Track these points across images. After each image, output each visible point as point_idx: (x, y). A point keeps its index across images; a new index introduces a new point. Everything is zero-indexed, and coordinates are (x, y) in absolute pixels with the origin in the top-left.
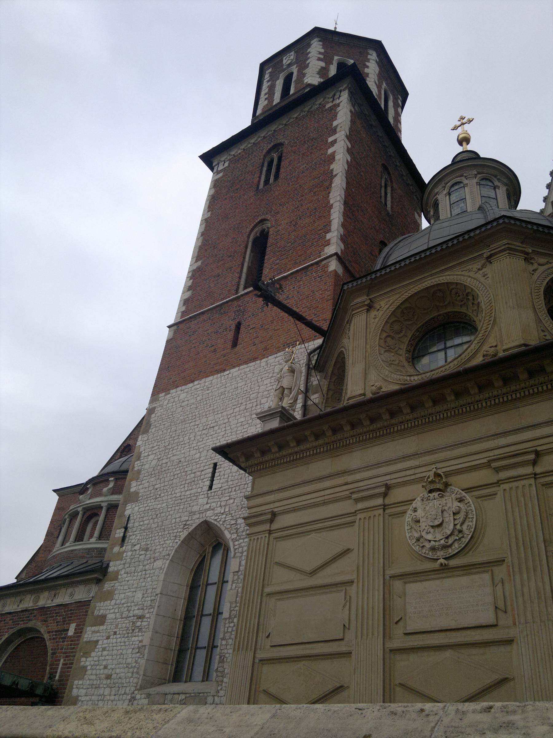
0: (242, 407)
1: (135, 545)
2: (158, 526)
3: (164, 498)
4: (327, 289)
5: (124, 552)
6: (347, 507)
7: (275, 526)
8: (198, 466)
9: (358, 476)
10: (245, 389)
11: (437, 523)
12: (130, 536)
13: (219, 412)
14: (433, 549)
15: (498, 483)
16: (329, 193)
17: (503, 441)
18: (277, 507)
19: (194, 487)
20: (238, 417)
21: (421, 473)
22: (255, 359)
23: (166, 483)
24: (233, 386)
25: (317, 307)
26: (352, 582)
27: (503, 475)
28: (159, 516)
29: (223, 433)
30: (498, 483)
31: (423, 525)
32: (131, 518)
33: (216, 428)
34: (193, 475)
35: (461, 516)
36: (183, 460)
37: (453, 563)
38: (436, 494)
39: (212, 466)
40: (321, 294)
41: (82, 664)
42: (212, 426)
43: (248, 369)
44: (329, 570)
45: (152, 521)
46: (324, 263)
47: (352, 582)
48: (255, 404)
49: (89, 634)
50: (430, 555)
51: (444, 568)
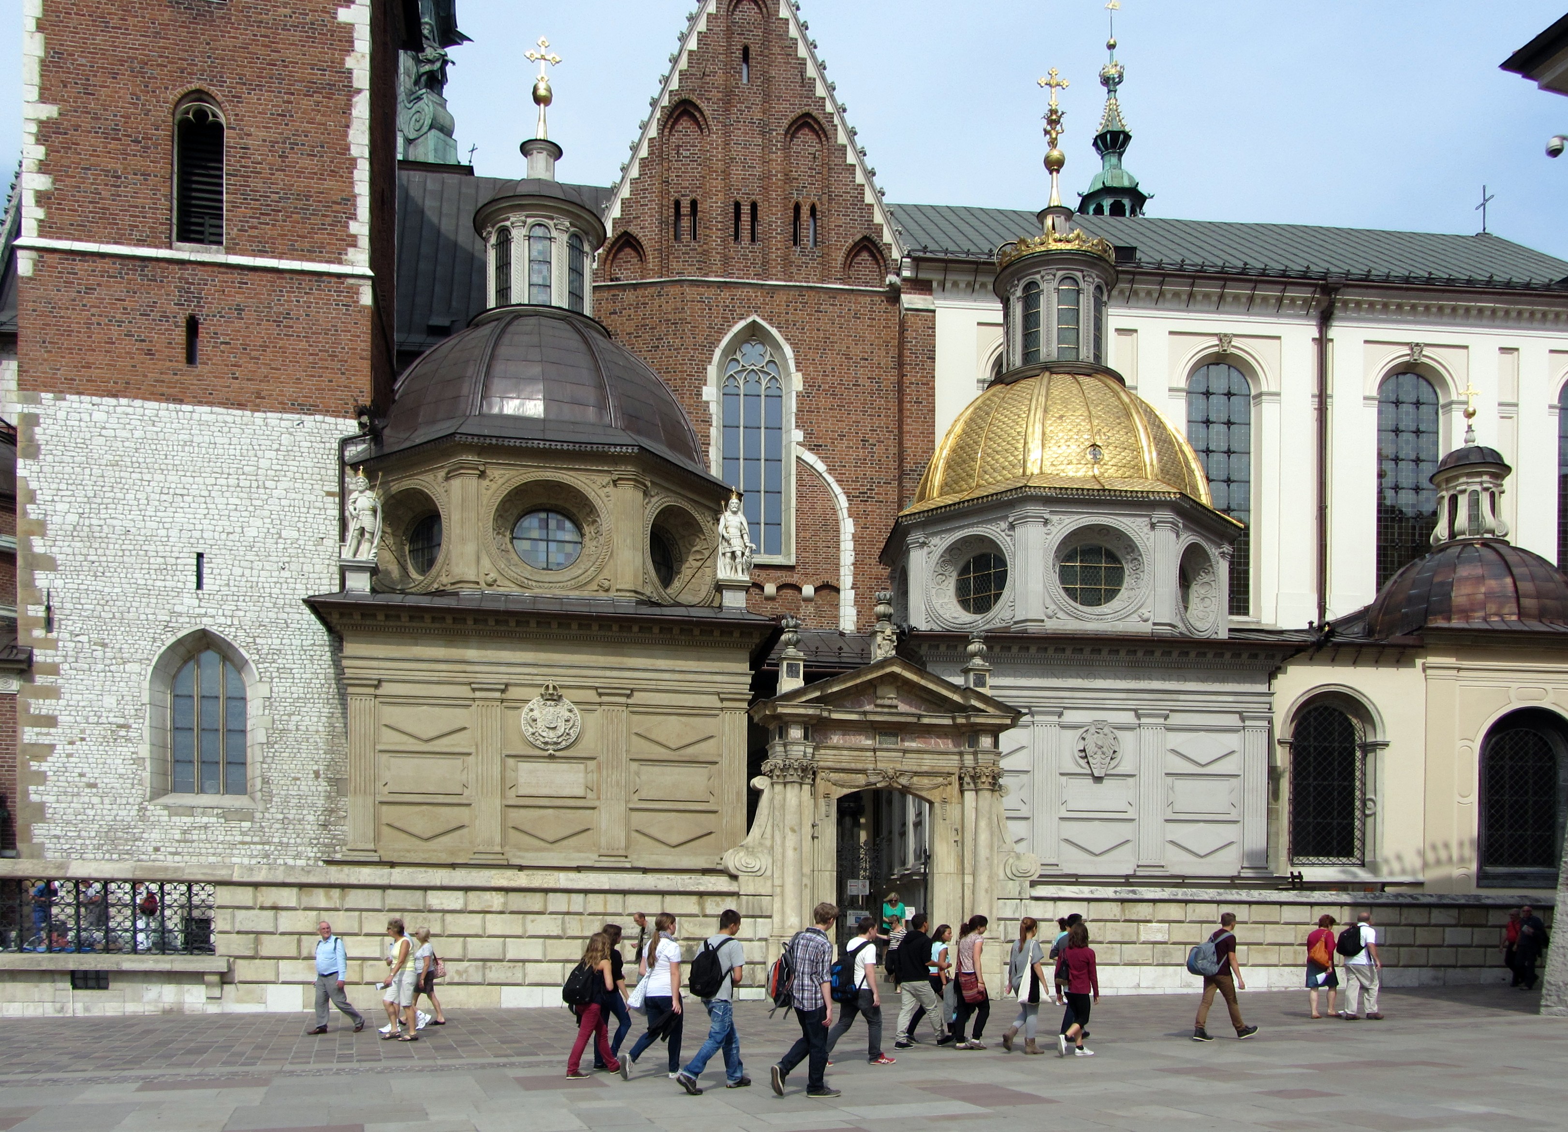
0: (232, 481)
1: (77, 635)
2: (114, 617)
3: (113, 580)
4: (359, 336)
5: (57, 640)
8: (168, 548)
10: (232, 452)
11: (552, 726)
12: (60, 620)
13: (188, 474)
14: (546, 743)
15: (600, 704)
17: (608, 673)
19: (169, 578)
20: (227, 494)
21: (539, 680)
22: (241, 406)
23: (110, 559)
24: (207, 439)
25: (346, 361)
26: (469, 754)
27: (605, 699)
28: (111, 603)
29: (206, 511)
30: (600, 704)
32: (53, 594)
33: (188, 499)
34: (162, 560)
35: (571, 723)
36: (133, 530)
37: (558, 754)
38: (553, 703)
39: (195, 556)
40: (351, 340)
41: (33, 768)
42: (178, 491)
43: (230, 419)
44: (445, 740)
45: (99, 608)
47: (469, 754)
48: (255, 484)
49: (29, 735)
51: (551, 757)
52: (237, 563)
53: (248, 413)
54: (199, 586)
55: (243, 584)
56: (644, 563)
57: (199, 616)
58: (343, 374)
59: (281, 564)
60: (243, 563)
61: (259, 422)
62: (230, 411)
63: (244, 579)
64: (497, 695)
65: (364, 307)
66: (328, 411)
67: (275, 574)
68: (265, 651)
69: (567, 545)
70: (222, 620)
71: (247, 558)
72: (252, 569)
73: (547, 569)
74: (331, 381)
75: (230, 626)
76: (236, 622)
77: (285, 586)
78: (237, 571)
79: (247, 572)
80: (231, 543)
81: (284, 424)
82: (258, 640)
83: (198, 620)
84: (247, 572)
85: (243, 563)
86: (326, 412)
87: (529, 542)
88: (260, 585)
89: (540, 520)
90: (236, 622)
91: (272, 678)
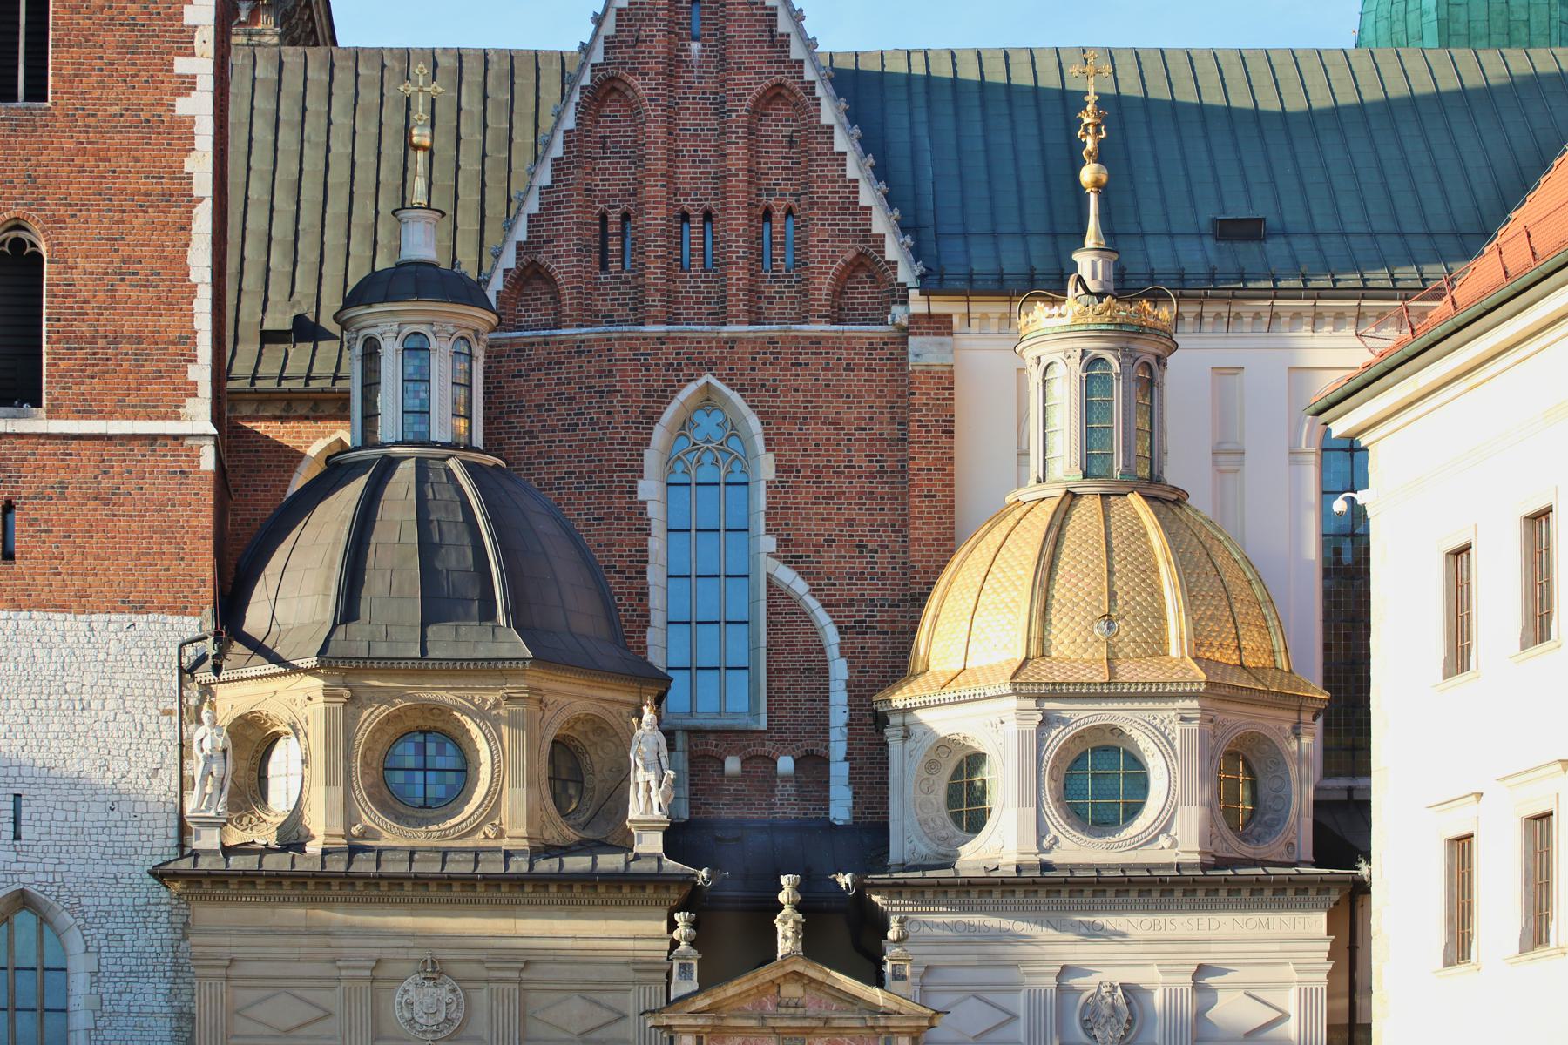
0: (52, 703)
6: (327, 969)
7: (233, 972)
9: (344, 942)
15: (487, 980)
16: (187, 245)
18: (237, 953)
22: (62, 608)
30: (487, 980)
31: (416, 1008)
46: (189, 442)
48: (78, 706)
50: (420, 1036)
52: (58, 805)
53: (70, 617)
54: (17, 837)
55: (66, 831)
56: (541, 798)
57: (17, 873)
58: (182, 559)
59: (110, 804)
60: (66, 806)
61: (83, 627)
62: (50, 615)
63: (67, 824)
64: (368, 973)
65: (206, 473)
66: (163, 608)
67: (103, 817)
68: (91, 914)
69: (448, 773)
70: (41, 877)
71: (70, 798)
72: (76, 811)
73: (425, 806)
74: (168, 570)
75: (51, 884)
76: (58, 879)
77: (114, 831)
78: (59, 816)
79: (71, 816)
80: (53, 781)
81: (112, 627)
82: (84, 901)
83: (16, 877)
84: (71, 816)
85: (66, 806)
86: (161, 609)
87: (402, 773)
88: (86, 831)
89: (417, 744)
90: (58, 879)
91: (100, 948)
